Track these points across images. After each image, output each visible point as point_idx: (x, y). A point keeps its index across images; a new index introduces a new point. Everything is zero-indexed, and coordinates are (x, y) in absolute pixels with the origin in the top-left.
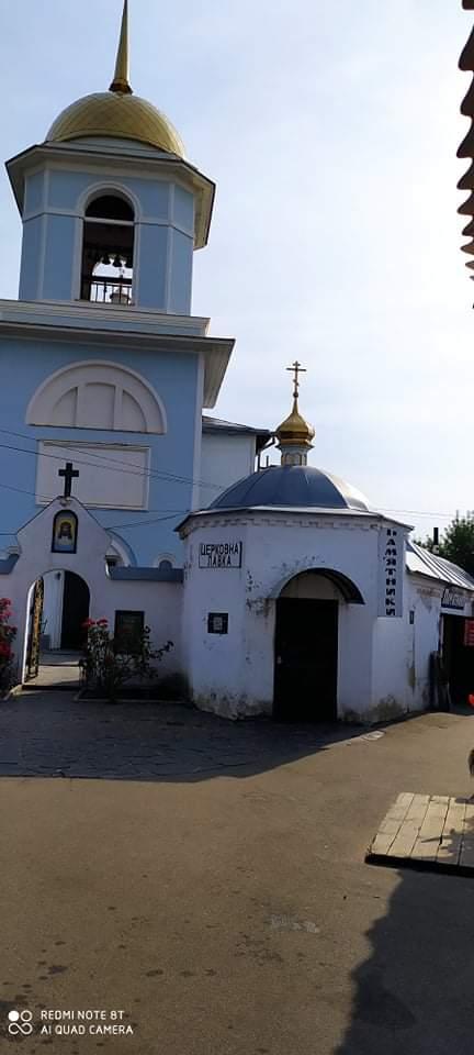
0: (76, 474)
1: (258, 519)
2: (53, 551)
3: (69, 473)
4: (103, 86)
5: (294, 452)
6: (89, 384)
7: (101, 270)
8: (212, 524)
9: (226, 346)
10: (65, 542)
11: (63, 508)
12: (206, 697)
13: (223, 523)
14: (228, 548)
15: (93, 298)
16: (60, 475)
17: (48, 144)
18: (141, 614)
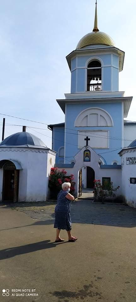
0: (89, 139)
2: (84, 161)
3: (87, 139)
4: (90, 30)
6: (90, 114)
7: (92, 82)
8: (130, 151)
9: (130, 99)
10: (87, 158)
11: (86, 149)
12: (131, 202)
15: (90, 90)
17: (77, 50)
18: (109, 178)
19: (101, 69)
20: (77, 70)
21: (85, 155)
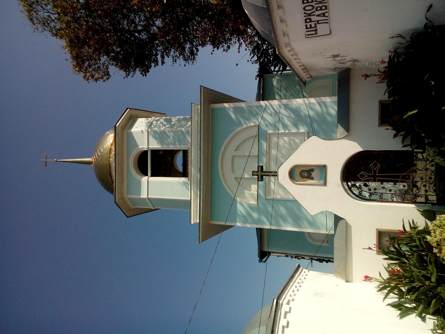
6: (233, 171)
7: (180, 168)
13: (281, 11)
16: (262, 180)
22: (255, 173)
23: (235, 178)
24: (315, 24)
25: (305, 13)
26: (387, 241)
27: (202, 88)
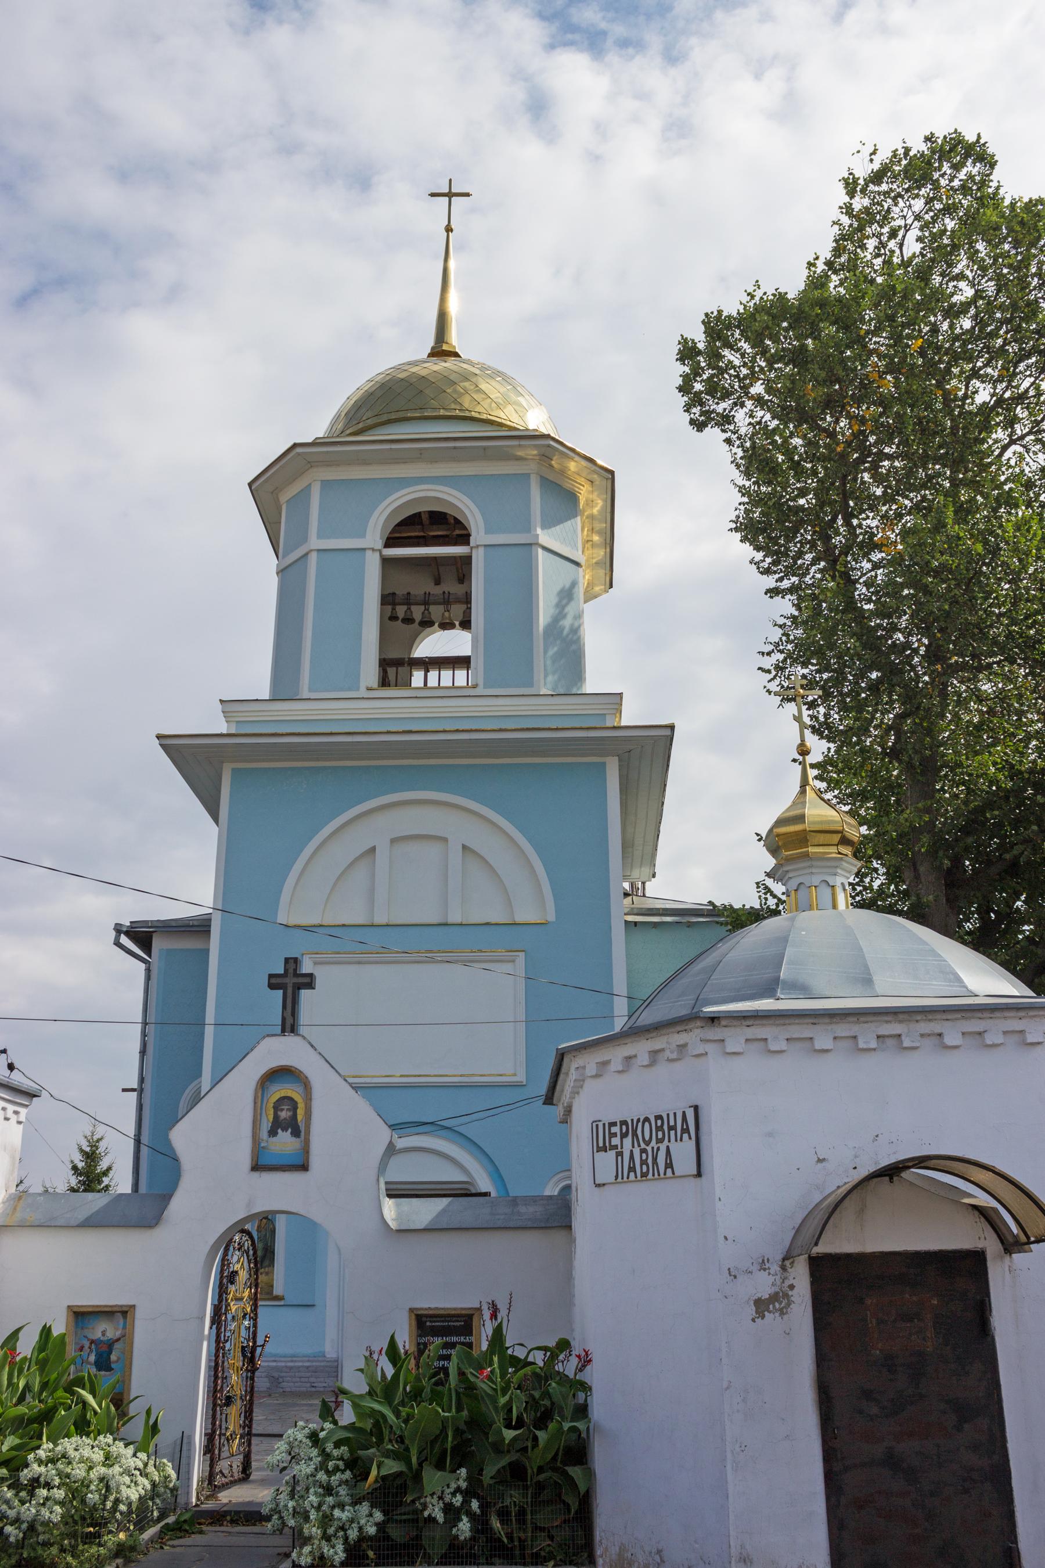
0: (309, 981)
1: (735, 1038)
2: (256, 1167)
5: (816, 880)
10: (285, 1143)
14: (663, 1126)
16: (272, 986)
19: (467, 560)
20: (314, 556)
21: (266, 1125)
22: (292, 966)
23: (373, 850)
24: (616, 1147)
25: (638, 1120)
26: (104, 1333)
27: (668, 732)
